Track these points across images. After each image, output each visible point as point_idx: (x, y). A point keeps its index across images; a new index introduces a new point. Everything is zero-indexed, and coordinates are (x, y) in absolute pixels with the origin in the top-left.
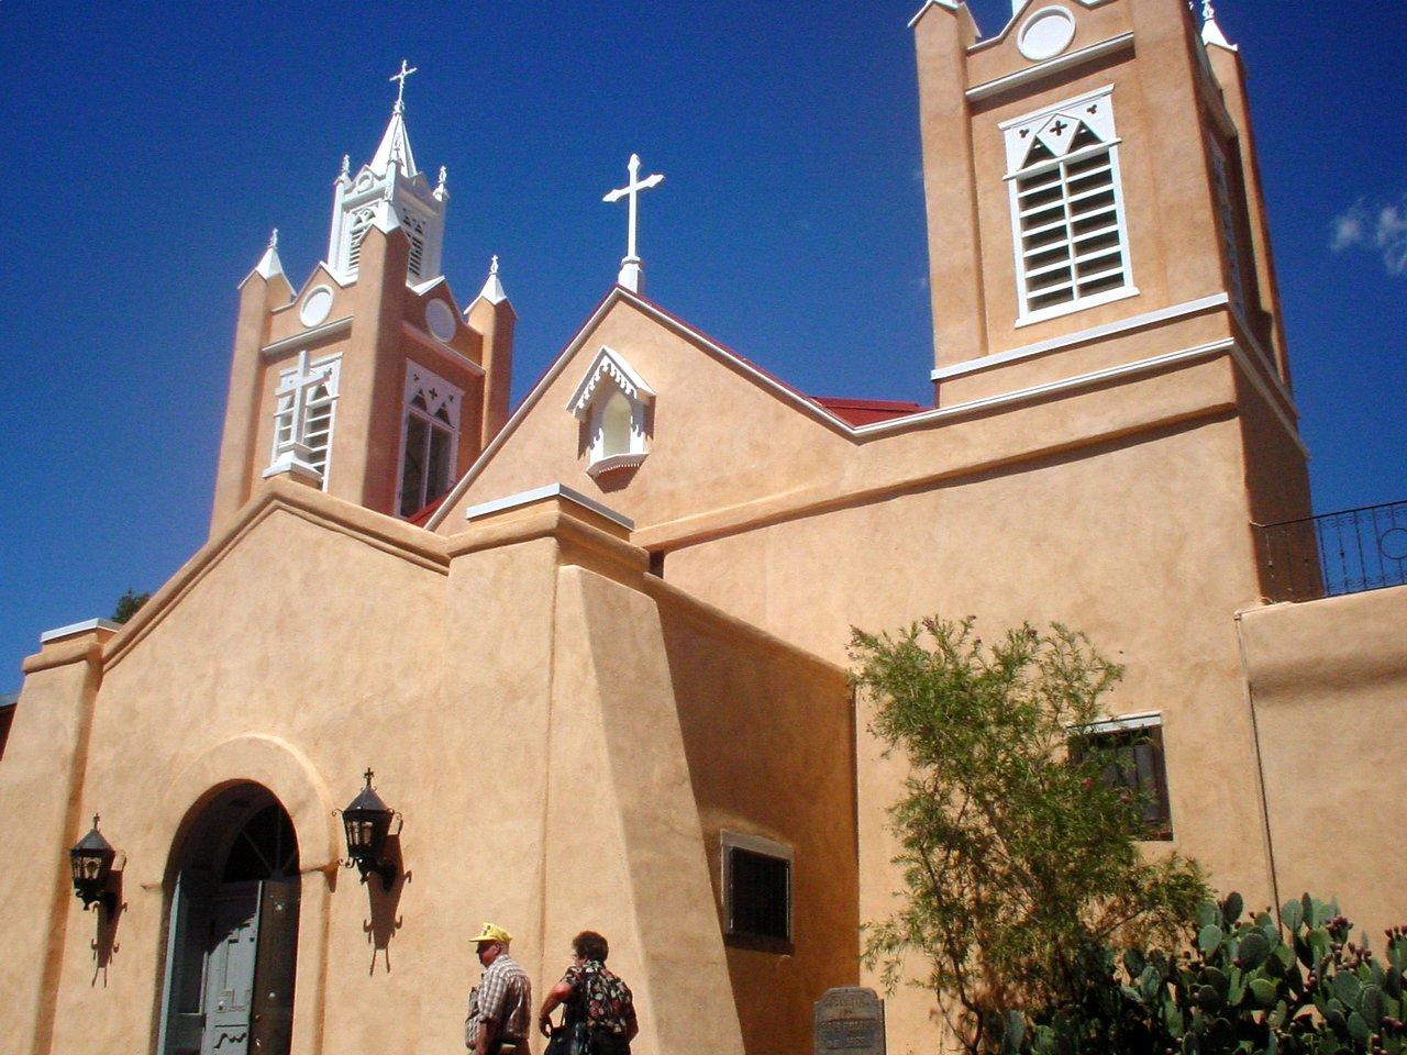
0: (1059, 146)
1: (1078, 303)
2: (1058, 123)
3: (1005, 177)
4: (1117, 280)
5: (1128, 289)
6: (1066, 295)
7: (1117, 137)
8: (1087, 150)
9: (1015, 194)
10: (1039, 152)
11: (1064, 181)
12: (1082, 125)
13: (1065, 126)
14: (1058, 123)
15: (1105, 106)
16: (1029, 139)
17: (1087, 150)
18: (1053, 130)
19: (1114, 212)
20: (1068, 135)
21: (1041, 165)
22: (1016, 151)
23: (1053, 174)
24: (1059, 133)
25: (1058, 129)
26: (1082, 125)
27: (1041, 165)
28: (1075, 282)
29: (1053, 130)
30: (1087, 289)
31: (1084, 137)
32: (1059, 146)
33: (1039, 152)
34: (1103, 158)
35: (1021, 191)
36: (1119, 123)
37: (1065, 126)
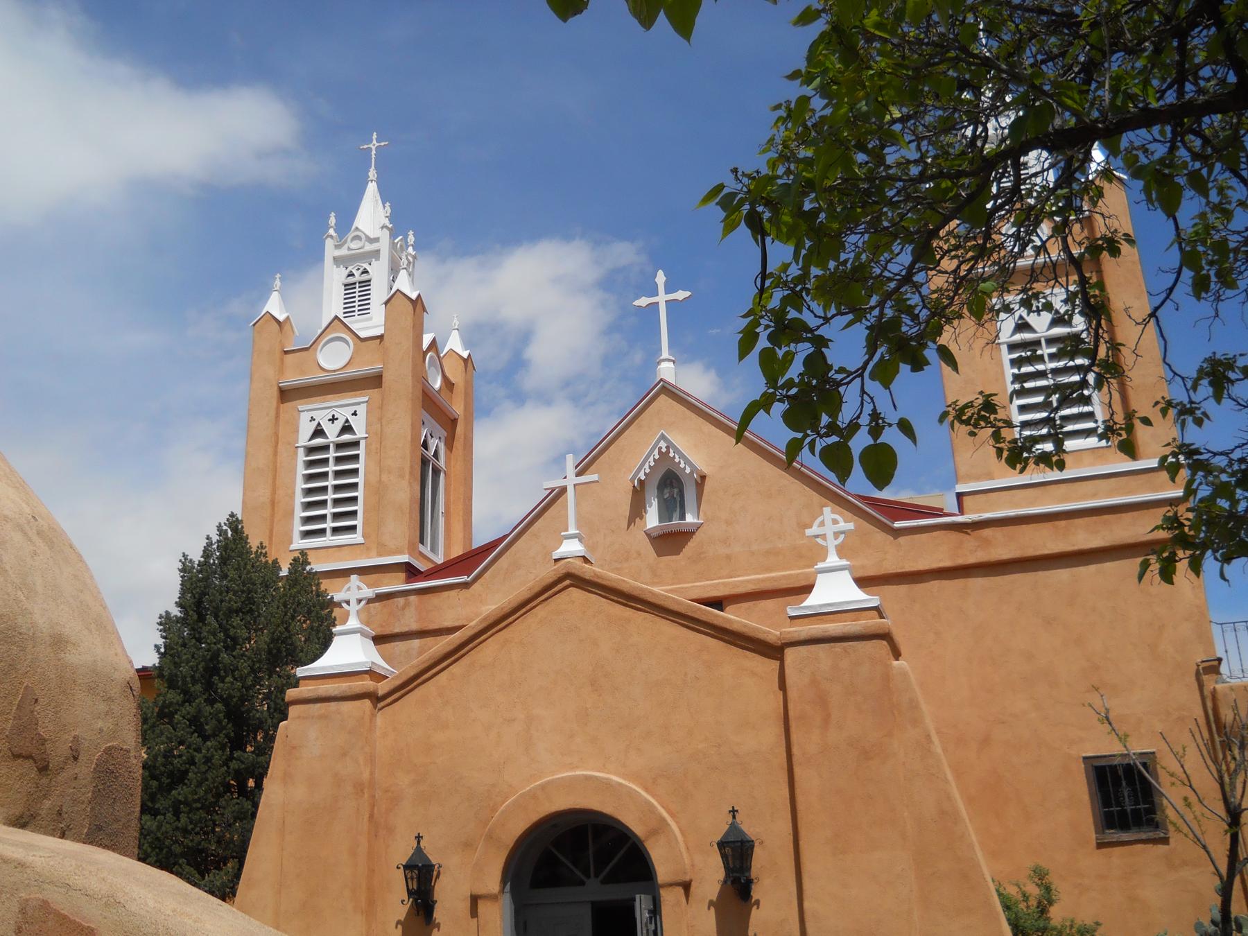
0: (332, 431)
1: (329, 540)
2: (333, 416)
3: (297, 445)
4: (352, 529)
5: (356, 538)
6: (322, 532)
7: (366, 433)
8: (347, 437)
9: (302, 457)
10: (319, 432)
11: (332, 454)
12: (347, 421)
13: (337, 419)
14: (333, 416)
15: (362, 410)
16: (315, 424)
17: (347, 437)
18: (329, 420)
19: (357, 483)
20: (339, 425)
21: (319, 441)
22: (306, 429)
23: (325, 448)
24: (333, 423)
25: (333, 419)
26: (347, 421)
27: (319, 441)
28: (329, 524)
29: (329, 420)
30: (336, 530)
31: (347, 428)
32: (332, 431)
33: (319, 432)
34: (355, 444)
35: (307, 456)
36: (369, 424)
37: (337, 419)
